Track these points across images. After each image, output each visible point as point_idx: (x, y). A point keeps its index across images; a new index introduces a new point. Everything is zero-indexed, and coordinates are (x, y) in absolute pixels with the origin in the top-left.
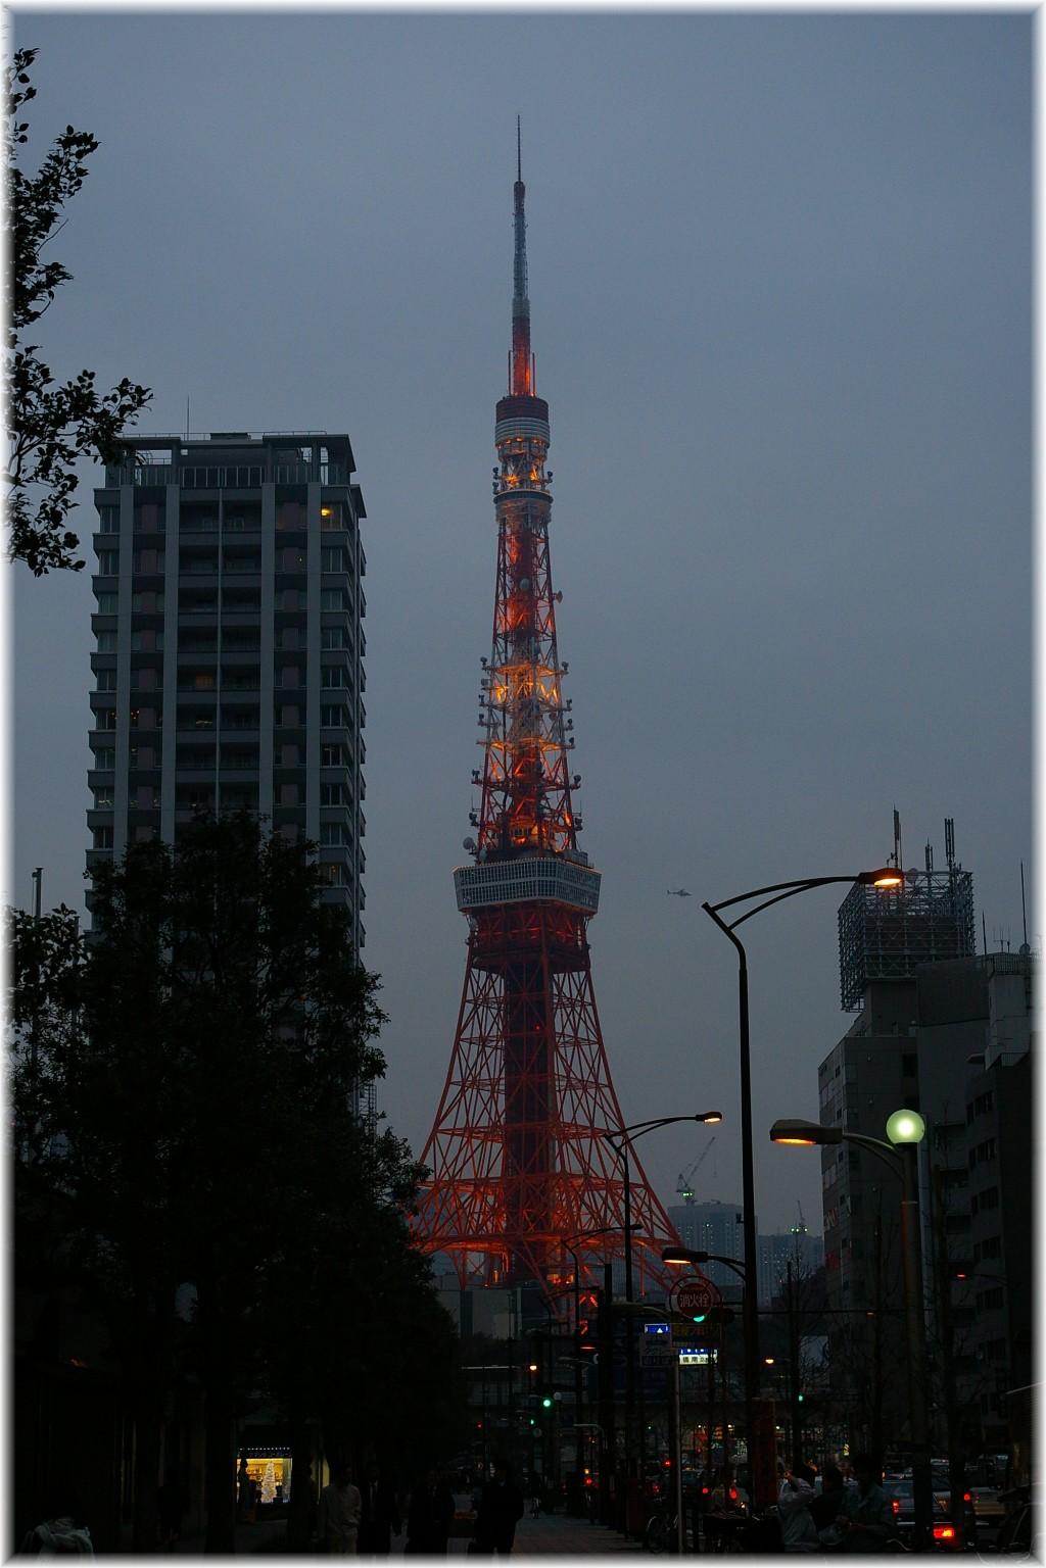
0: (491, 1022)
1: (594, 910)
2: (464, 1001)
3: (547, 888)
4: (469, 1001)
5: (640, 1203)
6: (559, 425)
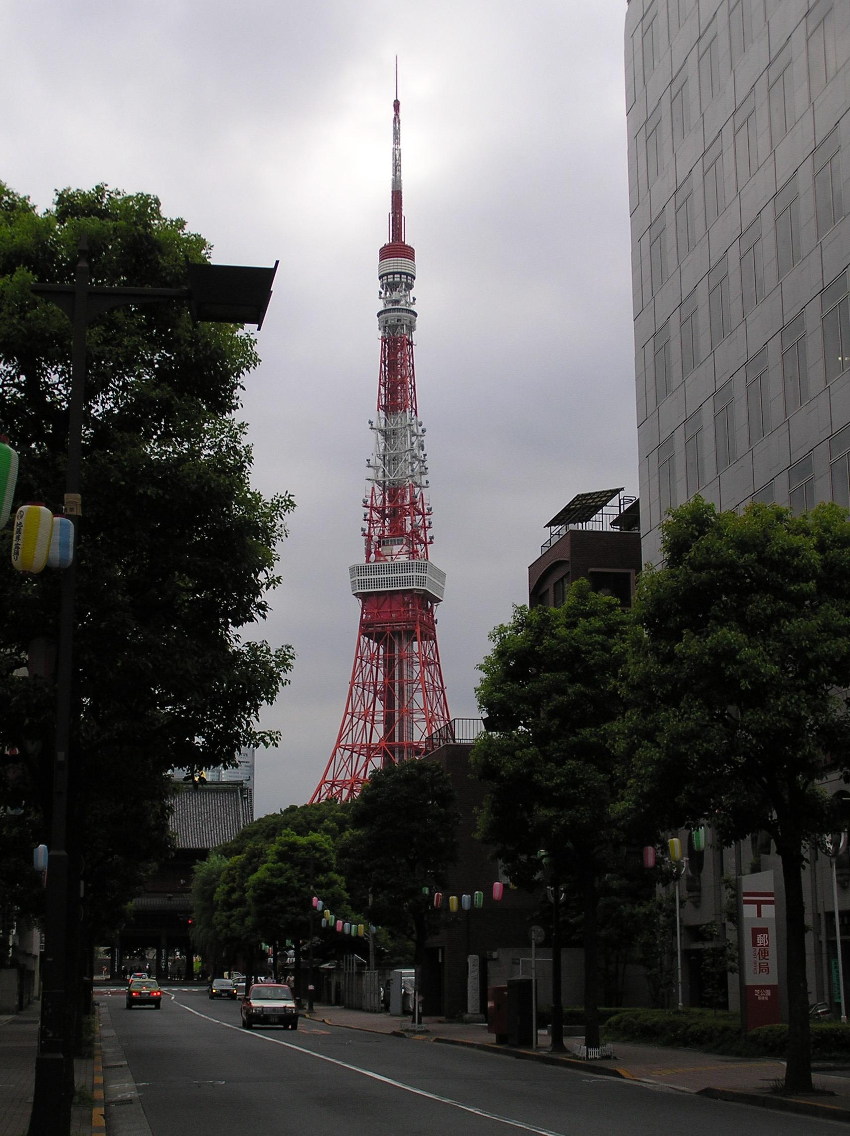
3: (421, 581)
6: (422, 266)
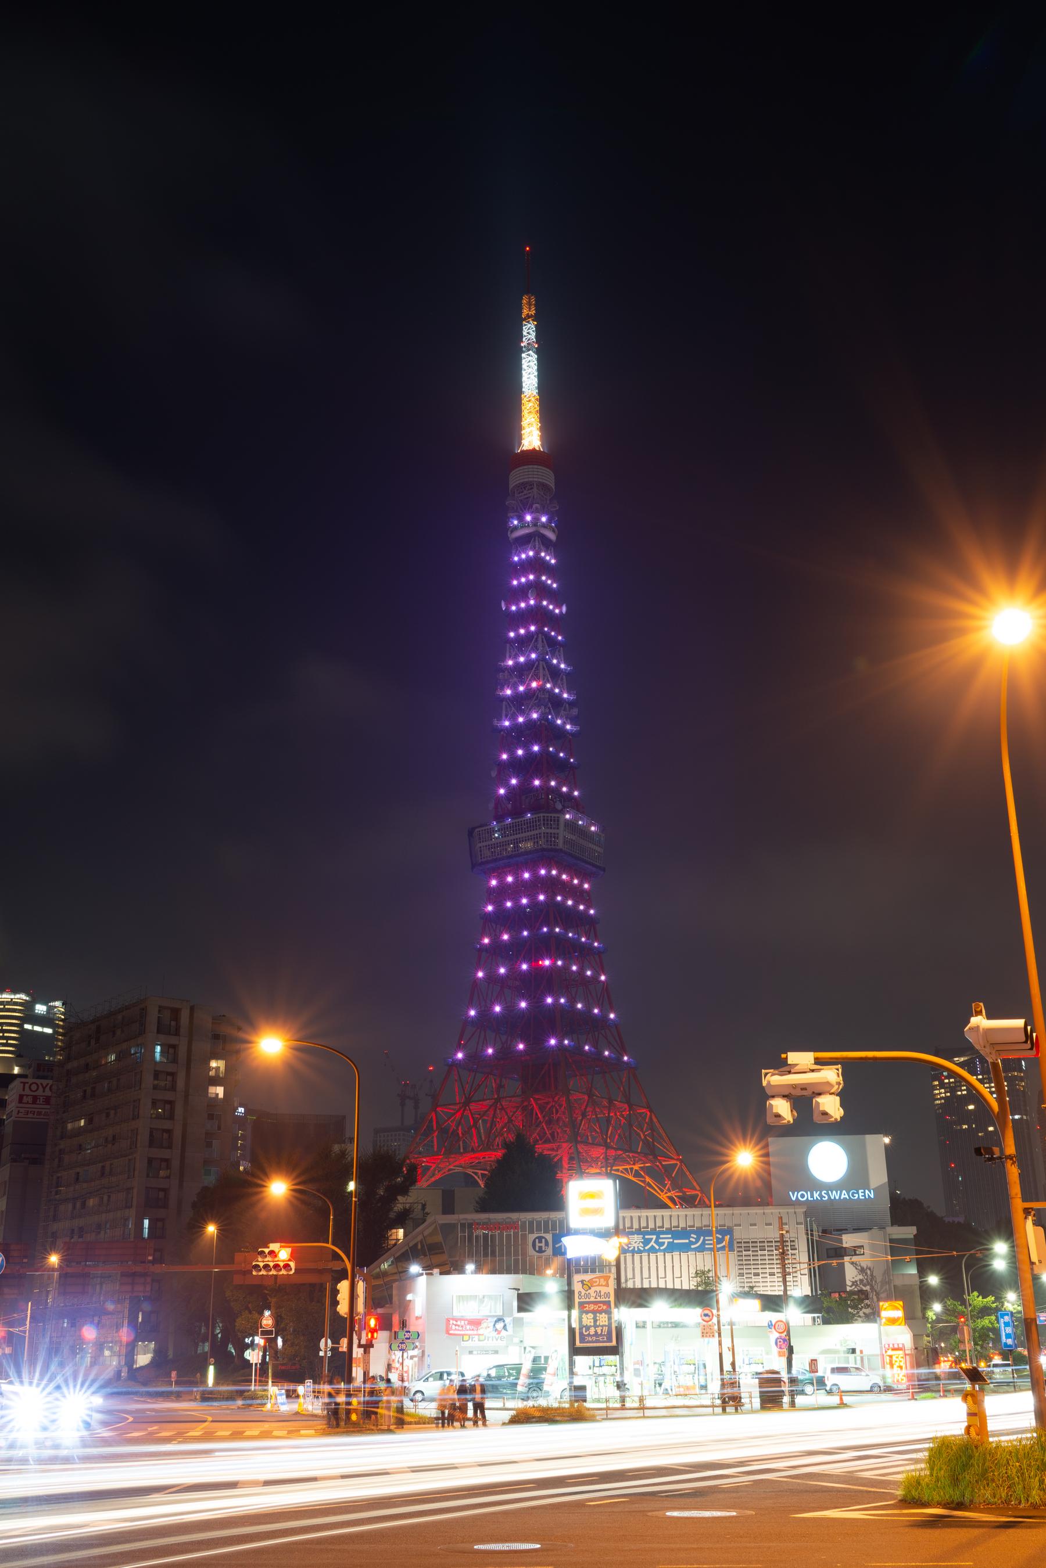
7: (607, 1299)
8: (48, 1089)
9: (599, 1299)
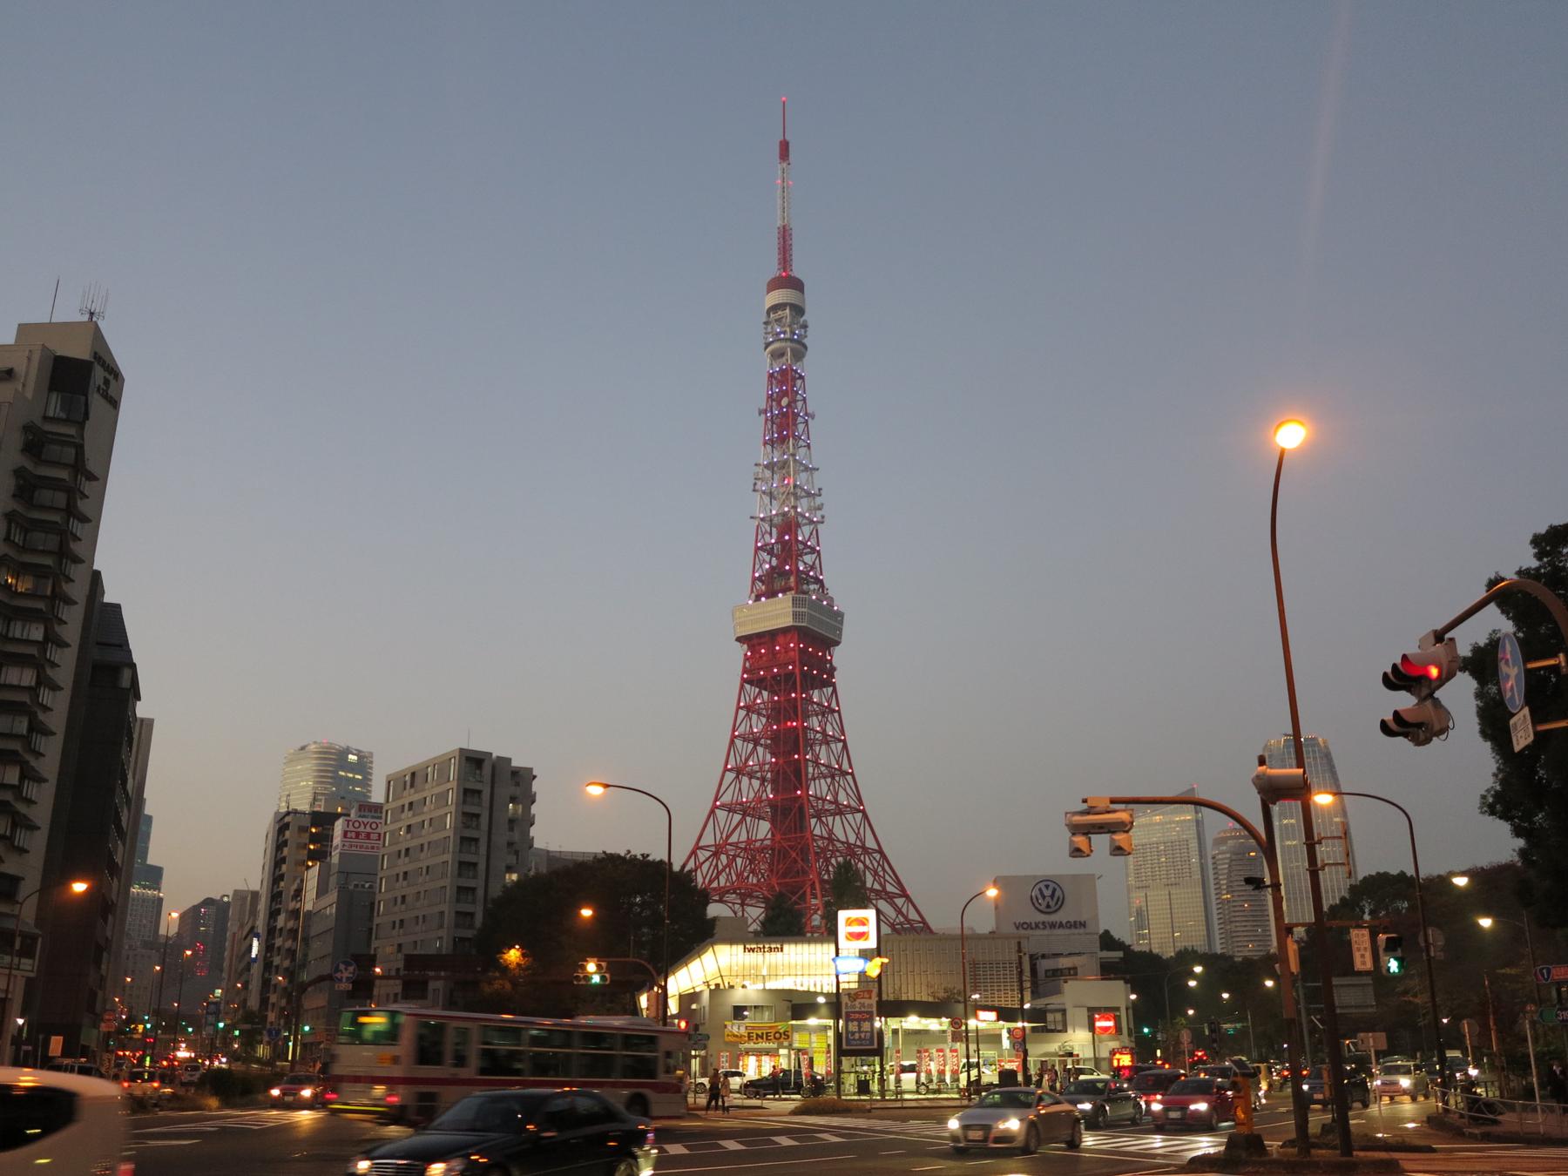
0: (757, 724)
1: (837, 639)
2: (739, 707)
4: (742, 708)
5: (876, 864)
7: (870, 1010)
8: (368, 826)
9: (863, 1009)
